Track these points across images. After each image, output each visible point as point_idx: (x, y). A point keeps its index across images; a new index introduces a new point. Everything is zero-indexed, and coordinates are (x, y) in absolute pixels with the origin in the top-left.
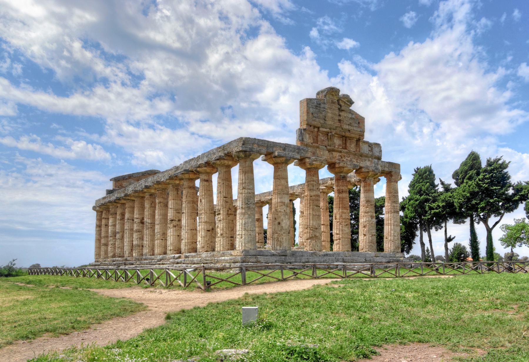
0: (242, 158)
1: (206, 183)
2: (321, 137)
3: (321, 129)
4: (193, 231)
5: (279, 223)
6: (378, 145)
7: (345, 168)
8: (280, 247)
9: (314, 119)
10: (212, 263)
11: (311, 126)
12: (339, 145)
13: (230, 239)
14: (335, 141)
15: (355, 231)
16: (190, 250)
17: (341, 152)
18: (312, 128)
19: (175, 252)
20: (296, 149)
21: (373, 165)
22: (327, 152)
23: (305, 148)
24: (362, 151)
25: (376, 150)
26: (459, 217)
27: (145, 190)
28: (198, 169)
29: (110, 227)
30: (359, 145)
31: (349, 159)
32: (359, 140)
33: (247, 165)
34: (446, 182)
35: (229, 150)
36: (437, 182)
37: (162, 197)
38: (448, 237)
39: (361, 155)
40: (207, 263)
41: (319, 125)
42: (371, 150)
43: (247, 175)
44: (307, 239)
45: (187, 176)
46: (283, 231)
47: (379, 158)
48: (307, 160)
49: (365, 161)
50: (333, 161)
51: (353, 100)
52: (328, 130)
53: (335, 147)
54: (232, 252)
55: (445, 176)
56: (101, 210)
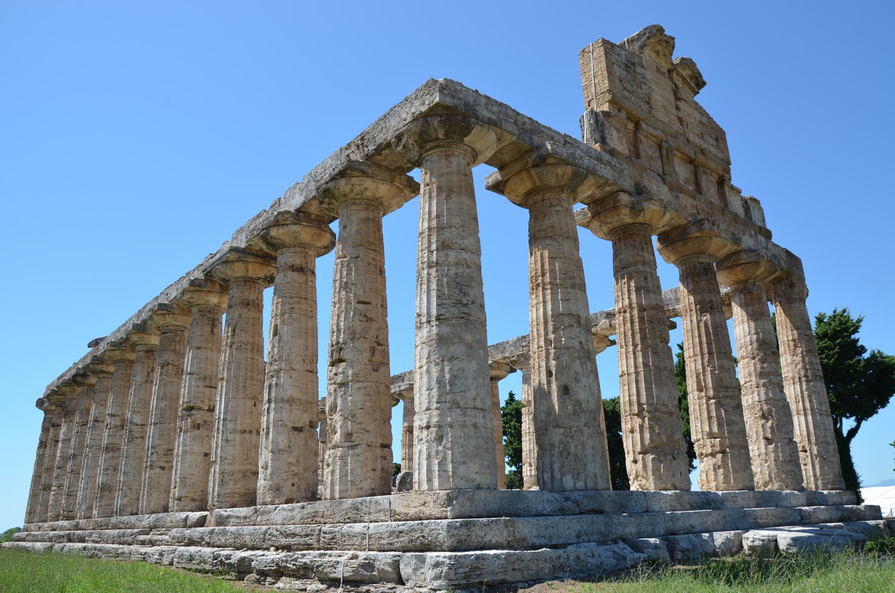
1: (296, 275)
4: (247, 436)
8: (576, 478)
10: (309, 547)
11: (619, 110)
12: (687, 181)
13: (379, 451)
16: (237, 498)
17: (694, 197)
18: (623, 114)
19: (193, 505)
25: (754, 213)
27: (135, 338)
28: (274, 232)
29: (60, 445)
32: (723, 181)
33: (454, 166)
35: (381, 138)
37: (174, 350)
40: (288, 548)
43: (454, 198)
44: (644, 452)
45: (239, 270)
46: (584, 418)
48: (624, 198)
51: (705, 78)
54: (396, 500)
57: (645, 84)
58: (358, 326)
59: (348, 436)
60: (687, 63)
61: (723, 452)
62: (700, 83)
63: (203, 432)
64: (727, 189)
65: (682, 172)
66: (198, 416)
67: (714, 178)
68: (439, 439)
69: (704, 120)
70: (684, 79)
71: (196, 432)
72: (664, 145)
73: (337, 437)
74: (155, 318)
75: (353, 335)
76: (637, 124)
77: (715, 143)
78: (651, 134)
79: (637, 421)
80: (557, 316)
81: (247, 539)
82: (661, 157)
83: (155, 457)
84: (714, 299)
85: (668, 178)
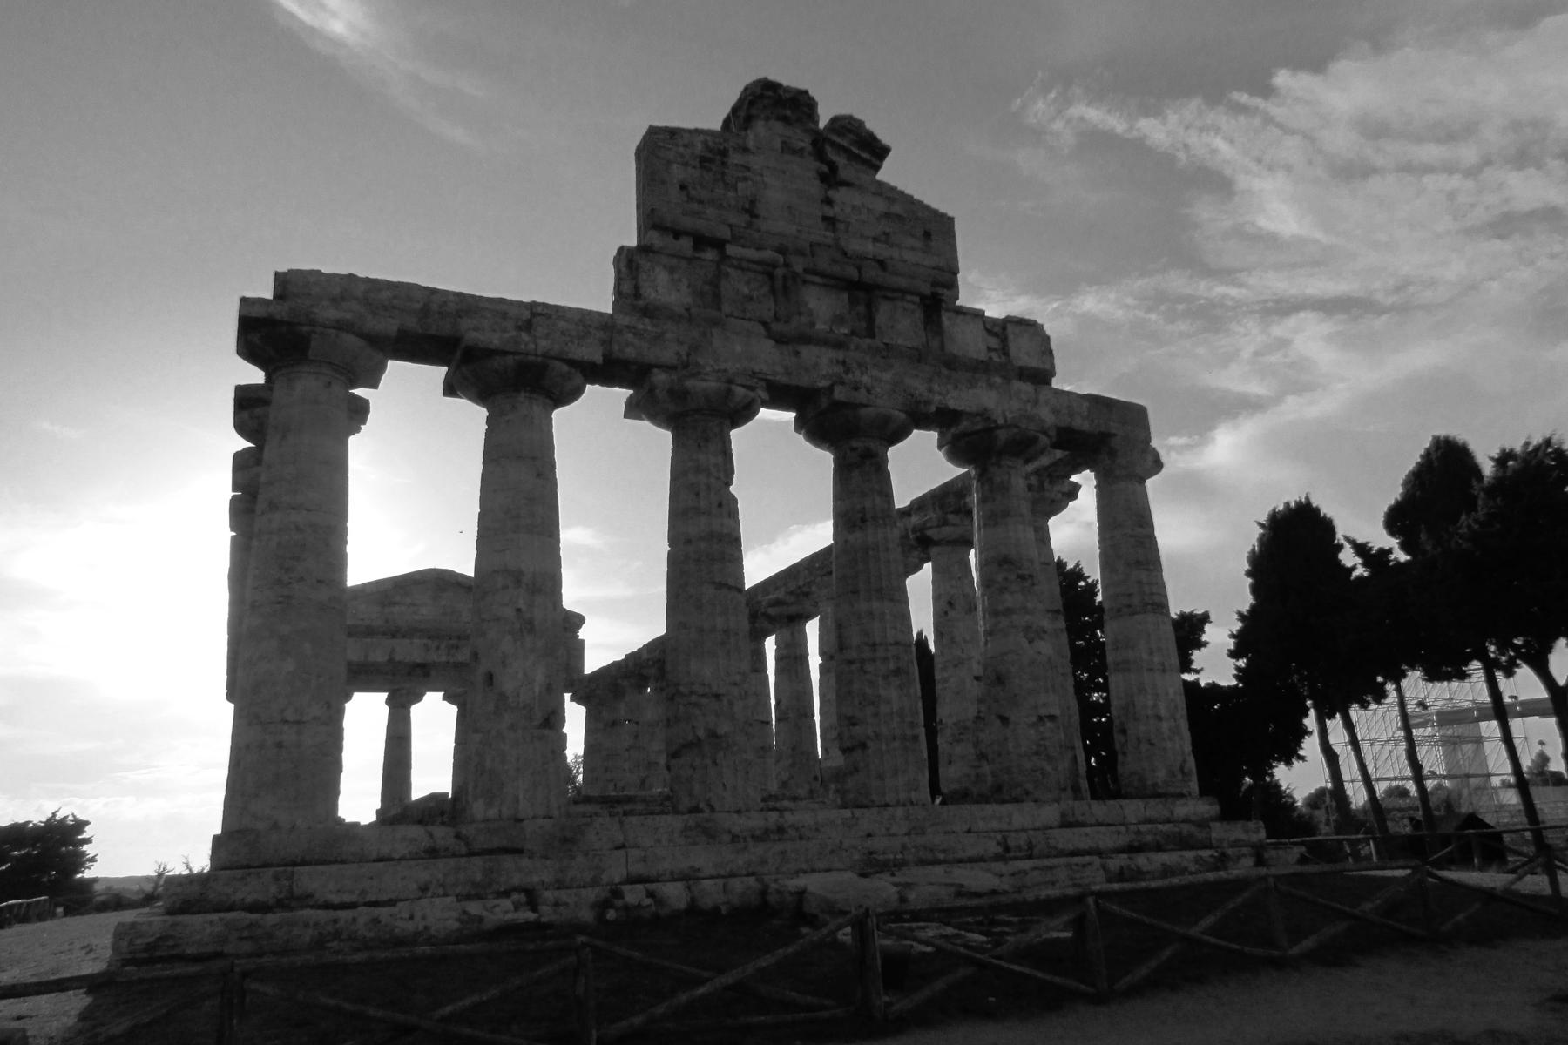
2: (737, 284)
3: (731, 250)
5: (490, 678)
7: (863, 412)
9: (695, 206)
12: (839, 320)
14: (813, 304)
17: (839, 345)
21: (1016, 405)
22: (771, 343)
23: (645, 325)
24: (953, 348)
30: (939, 324)
31: (887, 376)
39: (952, 363)
41: (724, 232)
42: (1005, 351)
47: (1042, 376)
49: (972, 384)
50: (804, 381)
52: (768, 254)
53: (813, 324)
55: (1361, 523)
57: (745, 179)
62: (876, 151)
69: (896, 208)
70: (846, 150)
72: (779, 272)
77: (918, 244)
78: (749, 261)
82: (773, 291)
84: (868, 504)
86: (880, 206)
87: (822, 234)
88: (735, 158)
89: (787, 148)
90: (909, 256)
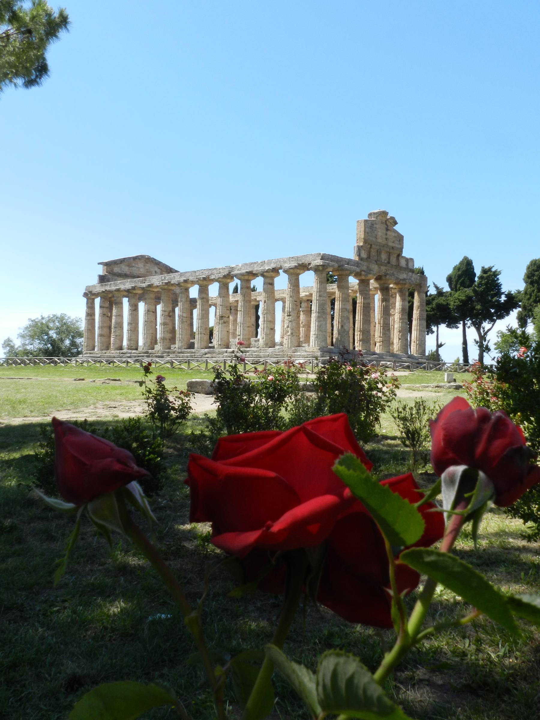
0: (320, 270)
3: (373, 246)
6: (412, 260)
12: (385, 260)
15: (332, 330)
17: (386, 266)
20: (357, 264)
26: (452, 323)
28: (265, 274)
32: (399, 255)
34: (440, 286)
36: (430, 283)
38: (439, 343)
42: (407, 264)
48: (363, 273)
56: (93, 297)
58: (295, 307)
59: (292, 333)
60: (392, 218)
61: (382, 342)
62: (396, 223)
63: (226, 324)
64: (400, 258)
65: (384, 256)
66: (225, 319)
67: (395, 256)
68: (317, 337)
71: (225, 324)
73: (289, 333)
74: (200, 282)
75: (293, 309)
76: (371, 245)
79: (359, 333)
80: (342, 309)
81: (262, 356)
83: (202, 330)
85: (378, 262)
86: (394, 234)
87: (384, 242)
88: (375, 226)
89: (382, 223)
90: (397, 246)
